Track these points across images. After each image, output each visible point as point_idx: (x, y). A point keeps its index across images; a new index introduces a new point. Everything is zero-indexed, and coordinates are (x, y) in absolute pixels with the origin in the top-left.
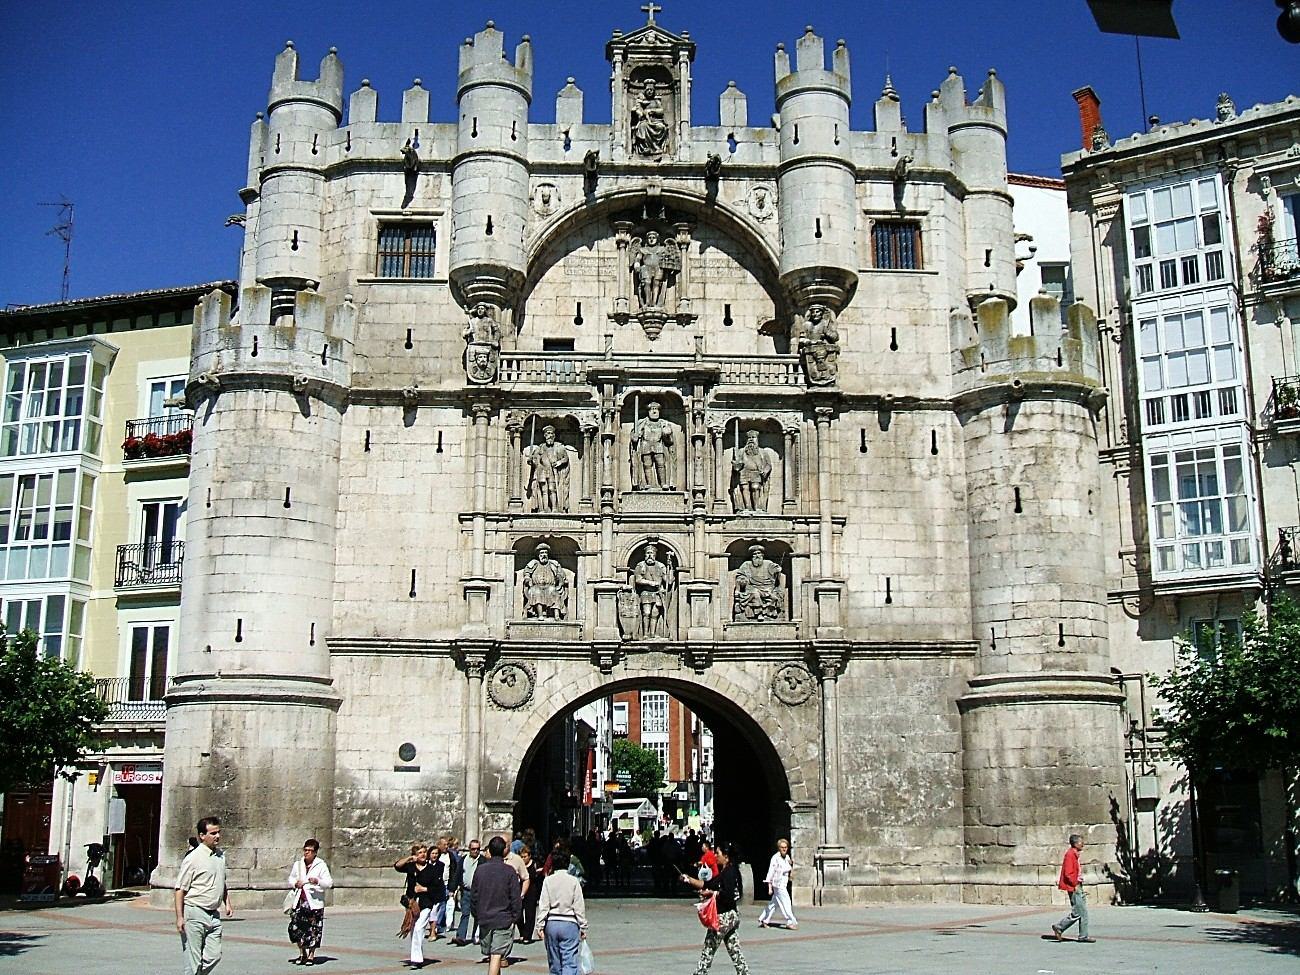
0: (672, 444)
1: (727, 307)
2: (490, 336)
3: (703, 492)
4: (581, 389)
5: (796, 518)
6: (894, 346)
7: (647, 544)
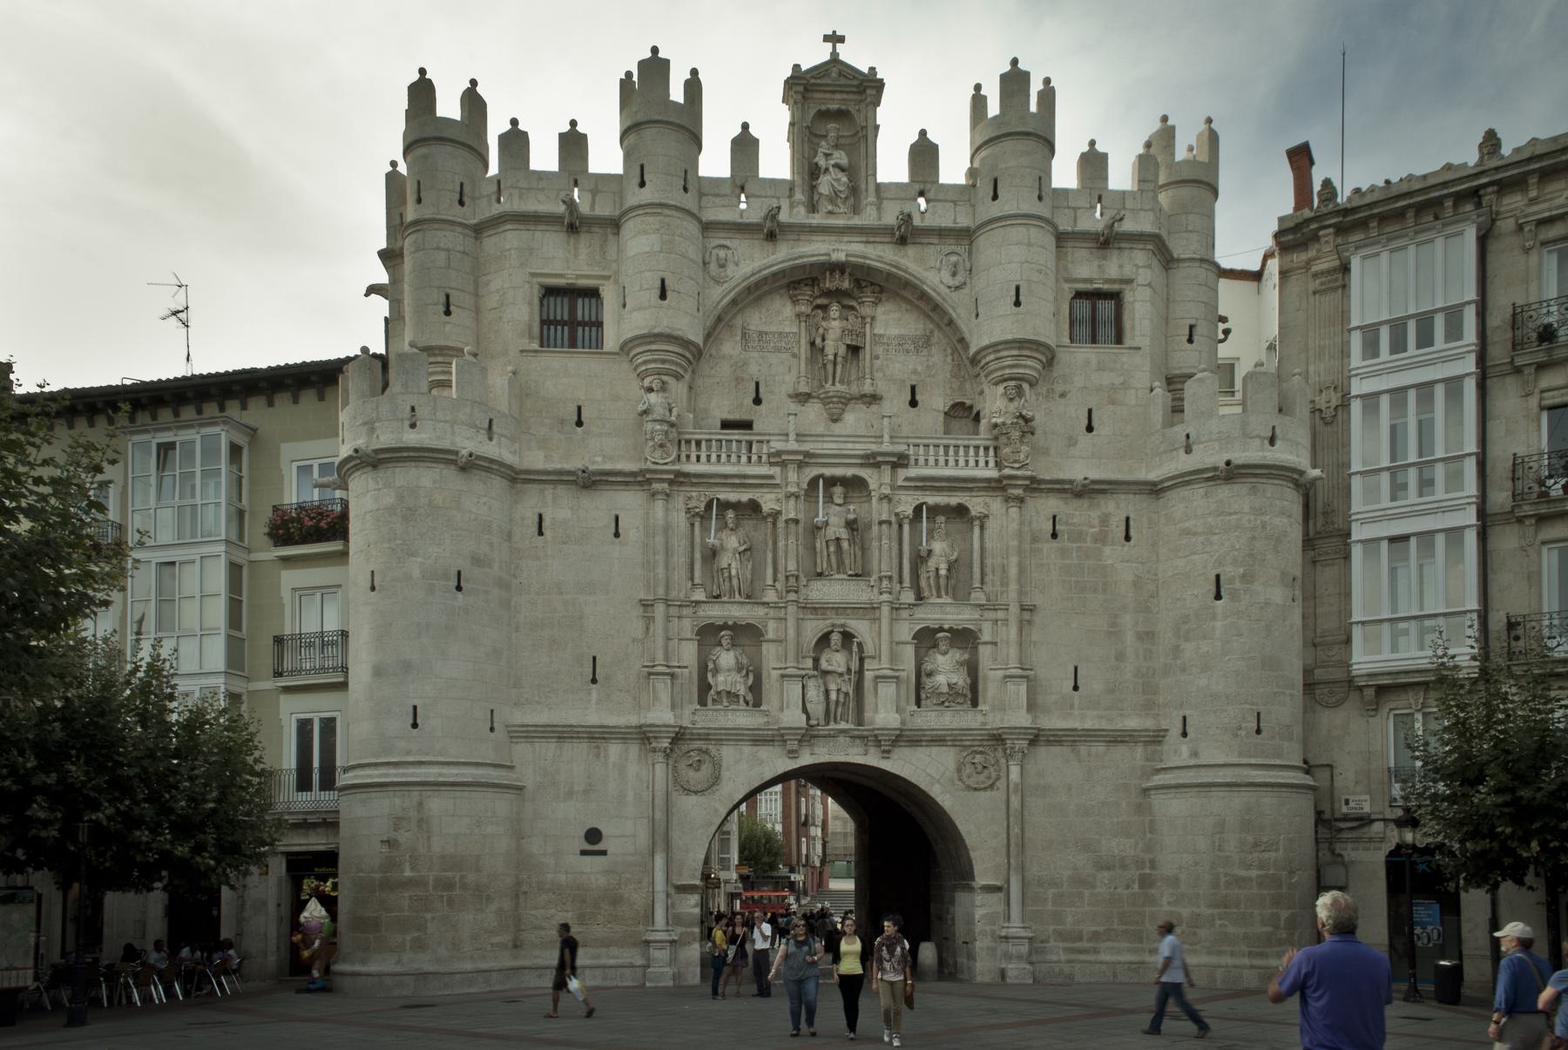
0: (857, 530)
4: (764, 470)
5: (983, 605)
6: (1090, 429)
7: (833, 631)
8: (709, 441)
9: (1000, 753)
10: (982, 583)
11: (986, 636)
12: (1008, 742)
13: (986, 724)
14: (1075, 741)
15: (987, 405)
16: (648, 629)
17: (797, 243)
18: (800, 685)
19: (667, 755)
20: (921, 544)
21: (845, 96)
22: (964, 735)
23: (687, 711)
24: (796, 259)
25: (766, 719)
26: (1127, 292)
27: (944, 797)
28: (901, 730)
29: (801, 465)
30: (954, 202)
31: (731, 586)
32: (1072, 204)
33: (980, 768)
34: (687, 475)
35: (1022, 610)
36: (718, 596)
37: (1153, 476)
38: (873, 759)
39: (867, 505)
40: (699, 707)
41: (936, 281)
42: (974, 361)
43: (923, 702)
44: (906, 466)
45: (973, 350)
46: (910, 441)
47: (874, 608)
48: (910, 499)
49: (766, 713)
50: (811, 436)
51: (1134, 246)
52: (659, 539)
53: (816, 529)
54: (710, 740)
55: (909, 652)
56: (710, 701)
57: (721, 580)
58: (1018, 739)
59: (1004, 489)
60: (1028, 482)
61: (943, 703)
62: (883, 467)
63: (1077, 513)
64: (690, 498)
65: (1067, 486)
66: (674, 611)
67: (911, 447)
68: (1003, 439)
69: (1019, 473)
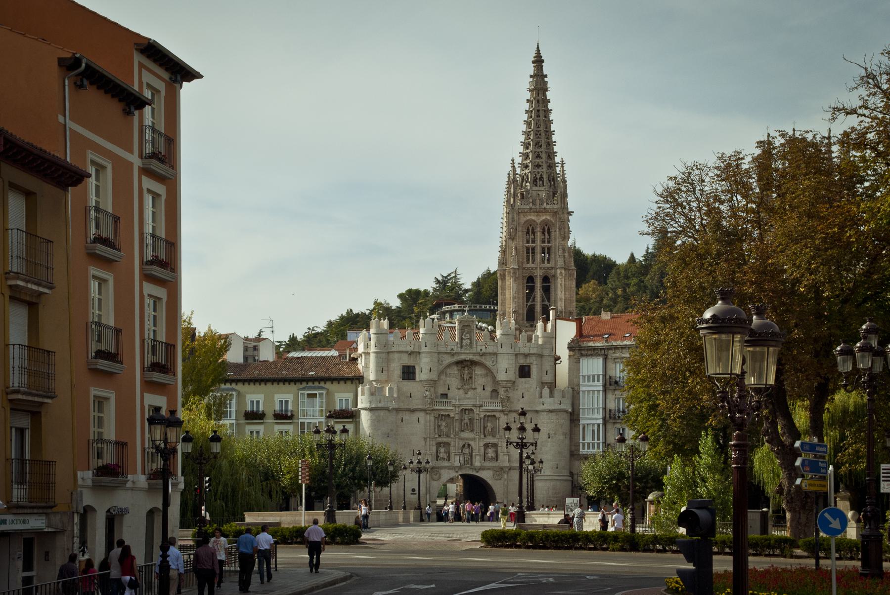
4: (451, 408)
6: (523, 397)
11: (500, 445)
27: (490, 481)
37: (537, 409)
38: (474, 473)
42: (497, 382)
52: (428, 424)
53: (462, 420)
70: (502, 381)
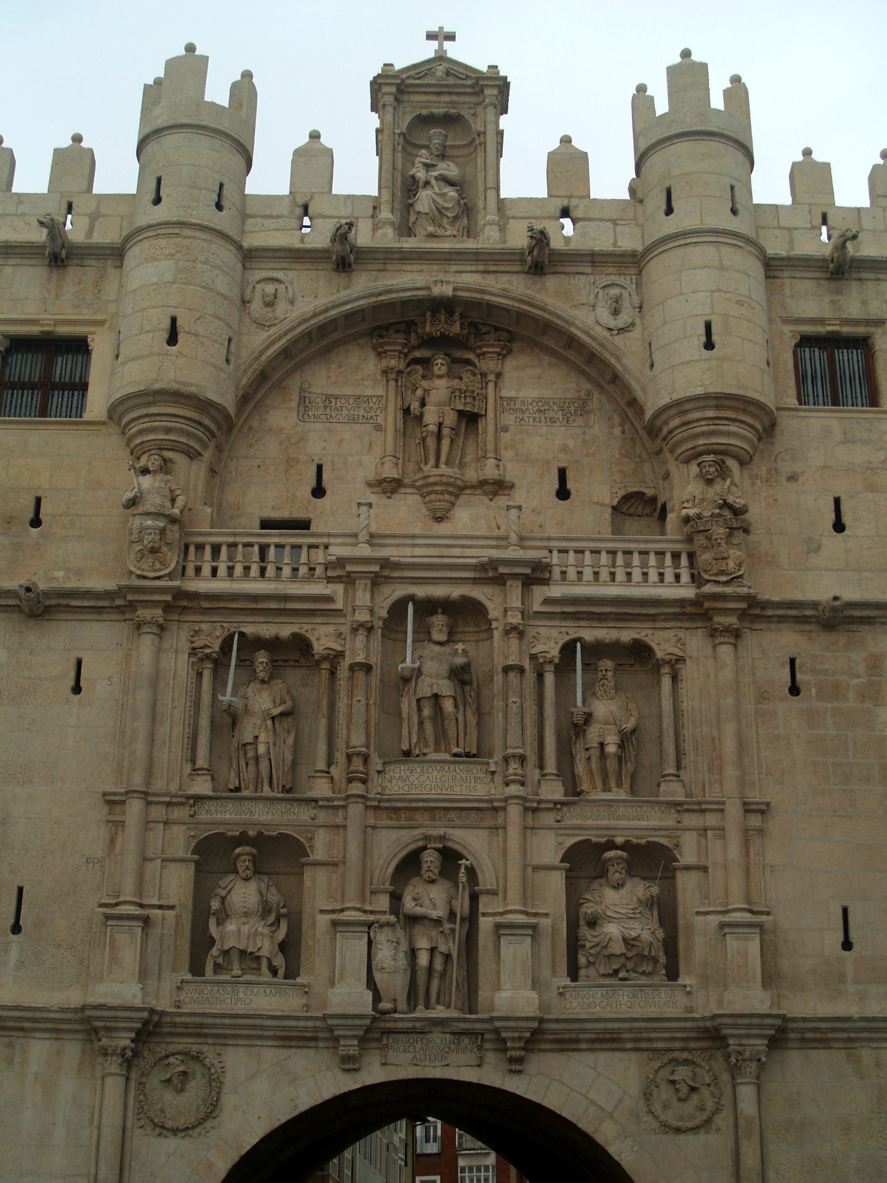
0: (470, 683)
1: (562, 474)
2: (168, 504)
3: (522, 759)
5: (680, 804)
6: (839, 526)
7: (425, 848)
8: (233, 546)
9: (719, 1065)
10: (678, 768)
11: (687, 857)
12: (731, 1041)
13: (690, 1009)
14: (850, 1040)
15: (676, 493)
16: (112, 841)
17: (382, 274)
18: (365, 940)
19: (129, 1061)
20: (575, 706)
21: (455, 98)
22: (655, 1030)
23: (170, 981)
24: (380, 294)
25: (304, 1001)
26: (877, 337)
28: (541, 1021)
29: (377, 582)
30: (614, 222)
31: (258, 774)
32: (783, 223)
33: (684, 1090)
34: (194, 596)
35: (747, 811)
36: (238, 789)
39: (487, 643)
40: (189, 977)
41: (590, 321)
42: (652, 431)
43: (582, 972)
44: (545, 582)
45: (648, 414)
46: (552, 544)
47: (495, 809)
48: (554, 633)
49: (306, 990)
50: (394, 537)
51: (881, 276)
52: (143, 696)
54: (206, 1036)
55: (556, 882)
56: (209, 967)
57: (243, 763)
58: (748, 1036)
59: (706, 616)
60: (743, 605)
61: (616, 972)
62: (509, 583)
63: (829, 655)
64: (197, 633)
65: (808, 613)
66: (158, 812)
67: (555, 553)
68: (700, 540)
69: (728, 590)
70: (679, 406)
